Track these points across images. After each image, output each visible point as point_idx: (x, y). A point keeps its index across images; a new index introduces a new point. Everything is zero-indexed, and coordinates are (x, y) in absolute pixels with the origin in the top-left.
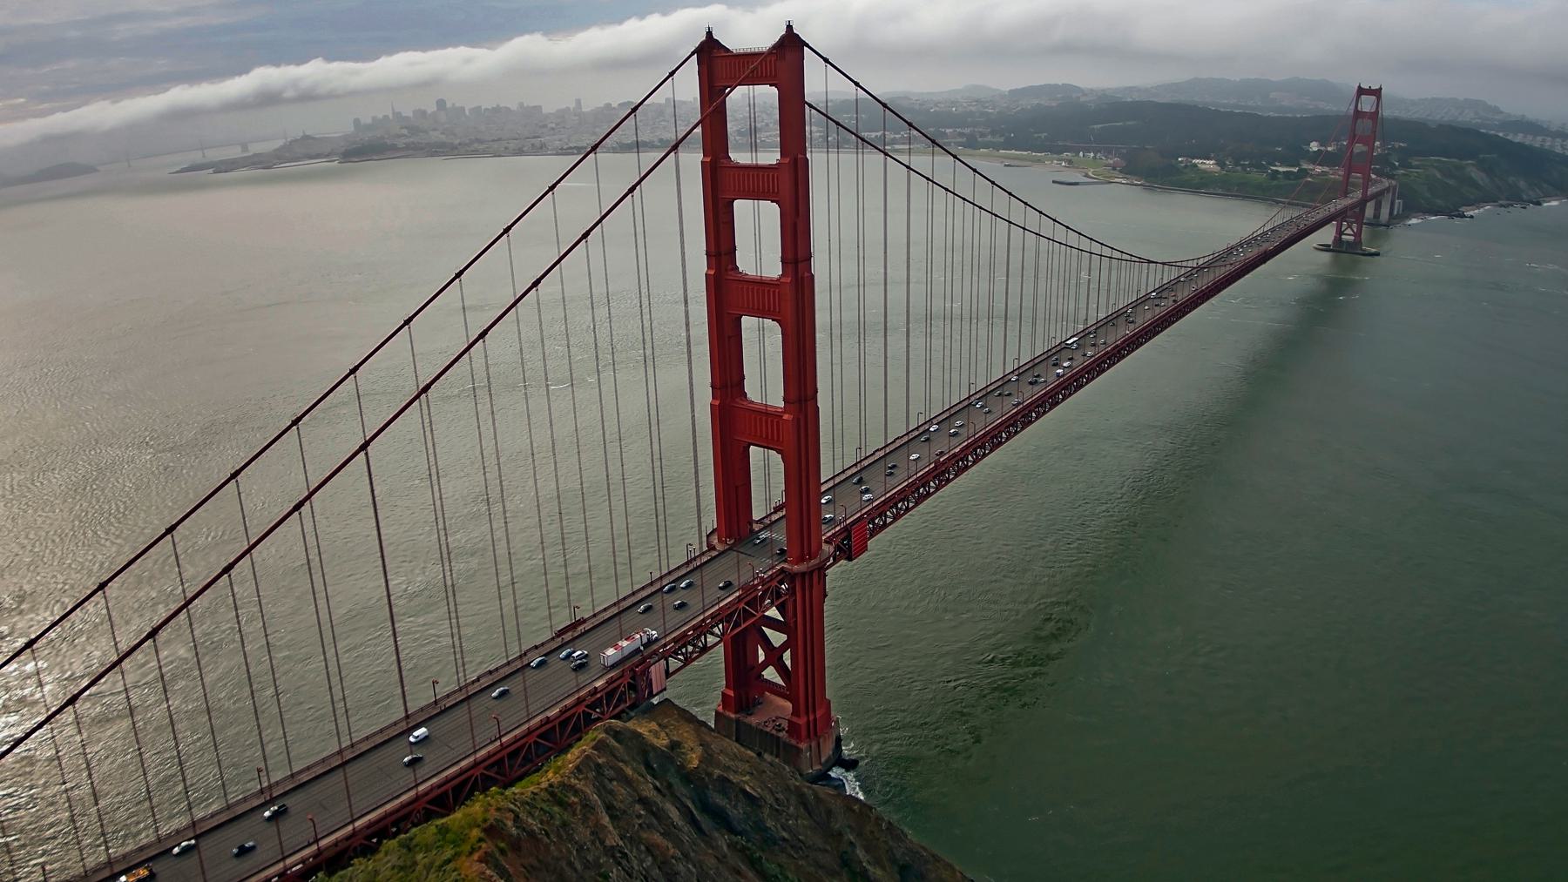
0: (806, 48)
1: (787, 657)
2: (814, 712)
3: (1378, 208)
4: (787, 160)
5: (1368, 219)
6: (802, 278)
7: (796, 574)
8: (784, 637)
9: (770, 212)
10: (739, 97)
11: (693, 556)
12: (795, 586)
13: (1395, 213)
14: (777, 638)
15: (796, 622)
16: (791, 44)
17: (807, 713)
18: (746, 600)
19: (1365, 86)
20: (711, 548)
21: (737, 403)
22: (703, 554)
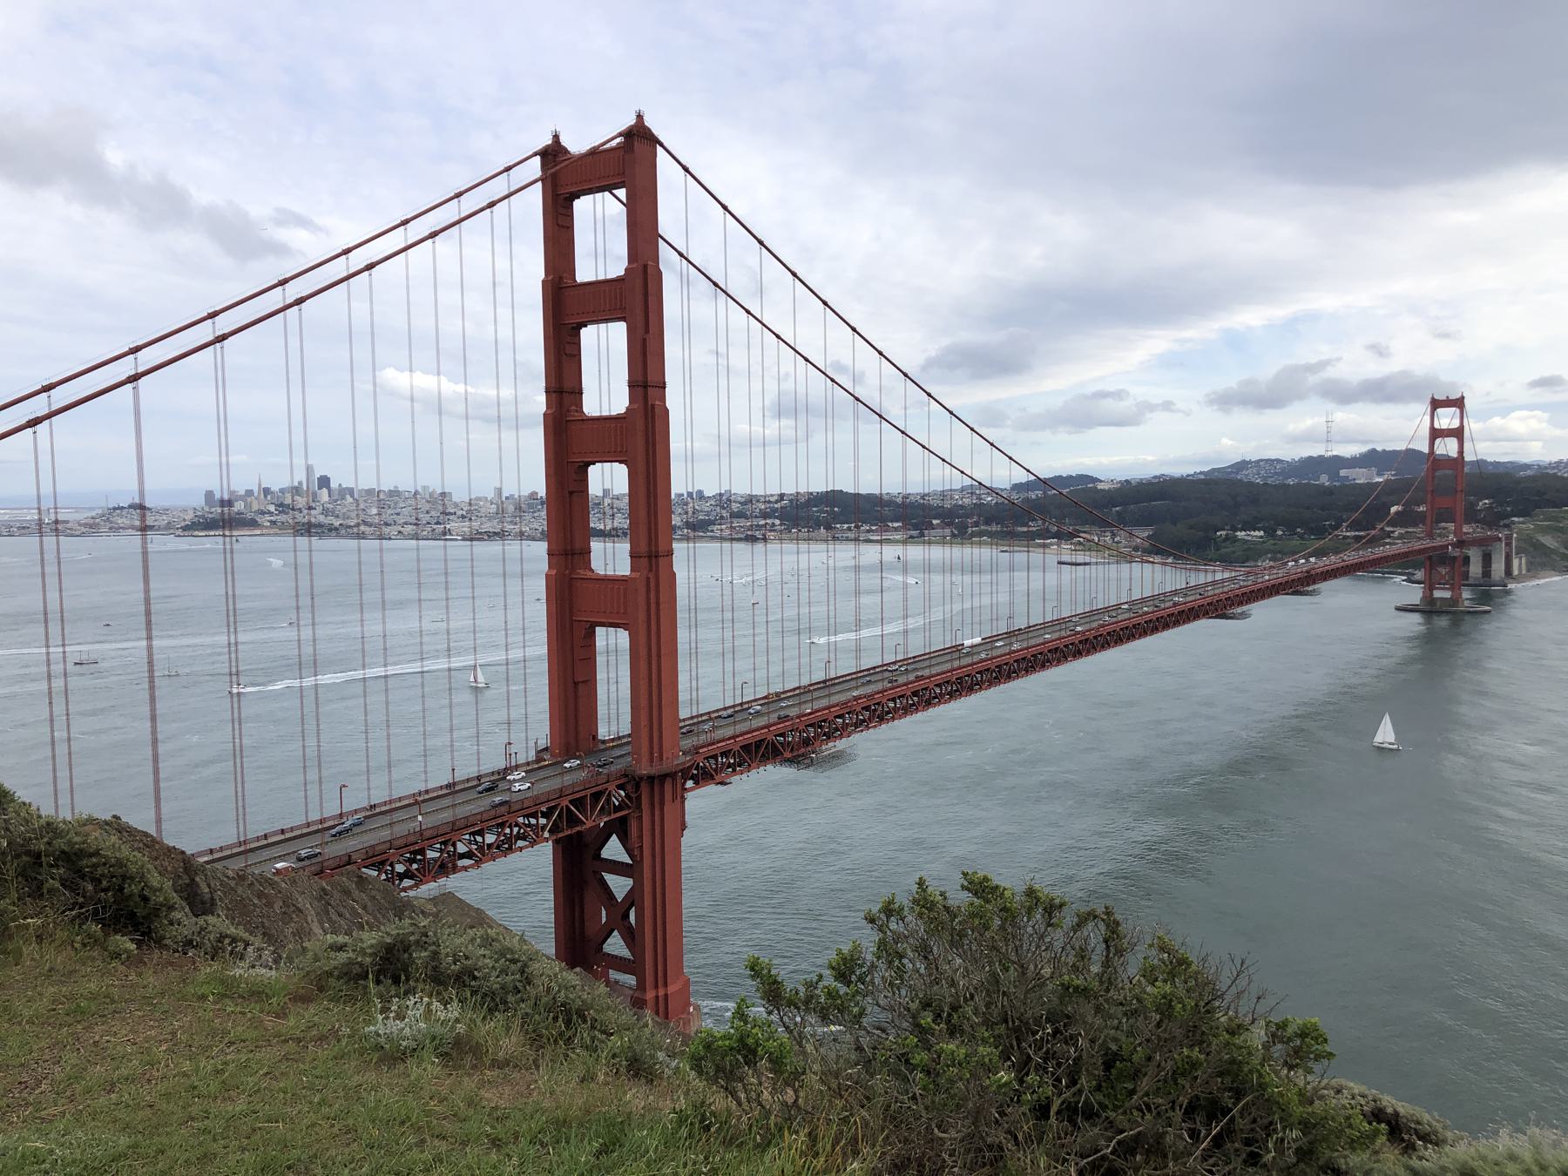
0: (659, 149)
2: (666, 985)
3: (1487, 560)
4: (634, 266)
5: (1476, 579)
6: (653, 406)
7: (641, 778)
8: (629, 882)
9: (616, 333)
11: (513, 764)
12: (641, 794)
13: (1516, 572)
14: (619, 885)
15: (641, 847)
16: (640, 140)
17: (656, 987)
18: (571, 798)
19: (1445, 398)
20: (539, 760)
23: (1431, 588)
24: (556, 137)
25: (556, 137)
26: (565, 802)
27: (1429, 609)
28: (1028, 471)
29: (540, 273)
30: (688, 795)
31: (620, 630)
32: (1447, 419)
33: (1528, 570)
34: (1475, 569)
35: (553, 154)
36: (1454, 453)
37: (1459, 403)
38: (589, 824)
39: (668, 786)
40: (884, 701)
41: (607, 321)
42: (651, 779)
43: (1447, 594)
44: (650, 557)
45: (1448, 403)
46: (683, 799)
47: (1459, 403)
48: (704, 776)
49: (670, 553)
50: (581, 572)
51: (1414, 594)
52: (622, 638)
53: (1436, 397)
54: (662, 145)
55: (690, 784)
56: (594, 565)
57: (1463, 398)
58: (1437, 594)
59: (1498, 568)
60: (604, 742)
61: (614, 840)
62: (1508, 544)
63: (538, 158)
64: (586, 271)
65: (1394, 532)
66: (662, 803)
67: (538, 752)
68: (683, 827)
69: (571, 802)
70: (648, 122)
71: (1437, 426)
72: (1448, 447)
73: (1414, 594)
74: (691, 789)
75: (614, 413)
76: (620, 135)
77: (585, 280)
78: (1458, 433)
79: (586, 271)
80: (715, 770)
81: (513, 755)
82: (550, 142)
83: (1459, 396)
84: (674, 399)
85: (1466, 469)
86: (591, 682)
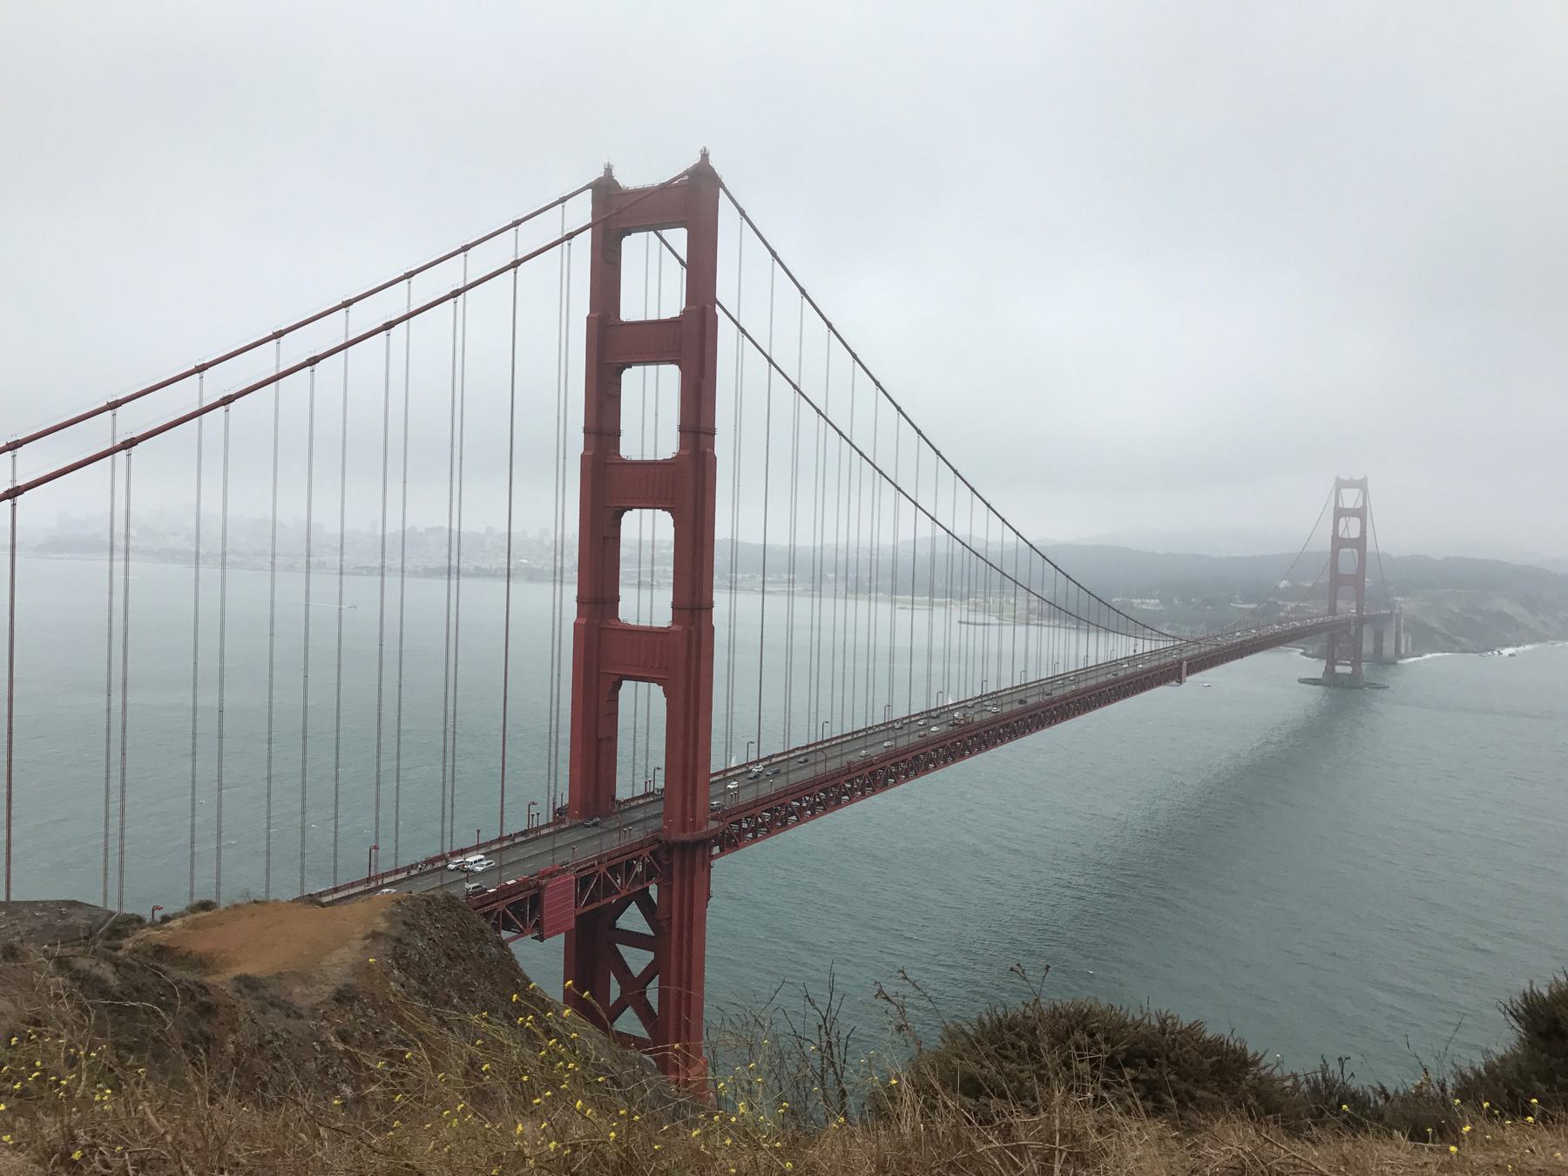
1: (652, 994)
3: (1379, 638)
4: (694, 307)
7: (675, 844)
9: (669, 377)
10: (636, 248)
13: (1403, 651)
14: (637, 960)
19: (1349, 478)
21: (610, 624)
22: (548, 825)
23: (1332, 663)
24: (609, 170)
25: (609, 170)
26: (603, 870)
27: (1330, 680)
28: (1018, 534)
29: (586, 310)
30: (715, 863)
31: (654, 685)
32: (1350, 499)
33: (1413, 649)
34: (1368, 647)
35: (605, 191)
36: (1355, 533)
37: (1362, 485)
38: (624, 893)
39: (699, 852)
40: (889, 765)
41: (657, 362)
42: (685, 846)
43: (1349, 670)
44: (692, 610)
45: (1351, 484)
46: (710, 867)
47: (1362, 485)
48: (730, 842)
49: (711, 606)
50: (612, 622)
51: (1317, 668)
52: (657, 690)
53: (1341, 477)
54: (722, 186)
55: (716, 850)
56: (621, 616)
57: (1365, 479)
58: (1339, 669)
59: (1388, 646)
60: (620, 803)
61: (633, 908)
62: (1398, 624)
63: (589, 191)
64: (632, 309)
65: (1286, 606)
66: (693, 871)
67: (555, 814)
68: (709, 896)
69: (608, 869)
70: (713, 162)
71: (1341, 506)
72: (1351, 528)
73: (1317, 668)
74: (718, 856)
75: (660, 458)
76: (686, 173)
77: (632, 320)
78: (1361, 513)
79: (632, 309)
80: (738, 835)
81: (536, 816)
82: (602, 175)
83: (1362, 477)
84: (722, 447)
85: (1370, 548)
86: (612, 739)
